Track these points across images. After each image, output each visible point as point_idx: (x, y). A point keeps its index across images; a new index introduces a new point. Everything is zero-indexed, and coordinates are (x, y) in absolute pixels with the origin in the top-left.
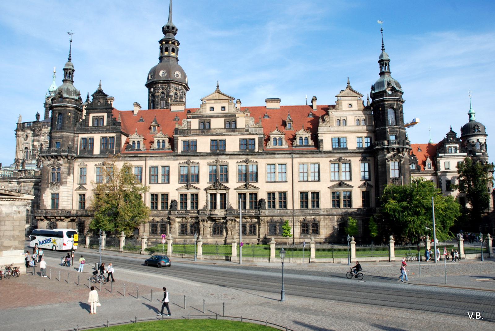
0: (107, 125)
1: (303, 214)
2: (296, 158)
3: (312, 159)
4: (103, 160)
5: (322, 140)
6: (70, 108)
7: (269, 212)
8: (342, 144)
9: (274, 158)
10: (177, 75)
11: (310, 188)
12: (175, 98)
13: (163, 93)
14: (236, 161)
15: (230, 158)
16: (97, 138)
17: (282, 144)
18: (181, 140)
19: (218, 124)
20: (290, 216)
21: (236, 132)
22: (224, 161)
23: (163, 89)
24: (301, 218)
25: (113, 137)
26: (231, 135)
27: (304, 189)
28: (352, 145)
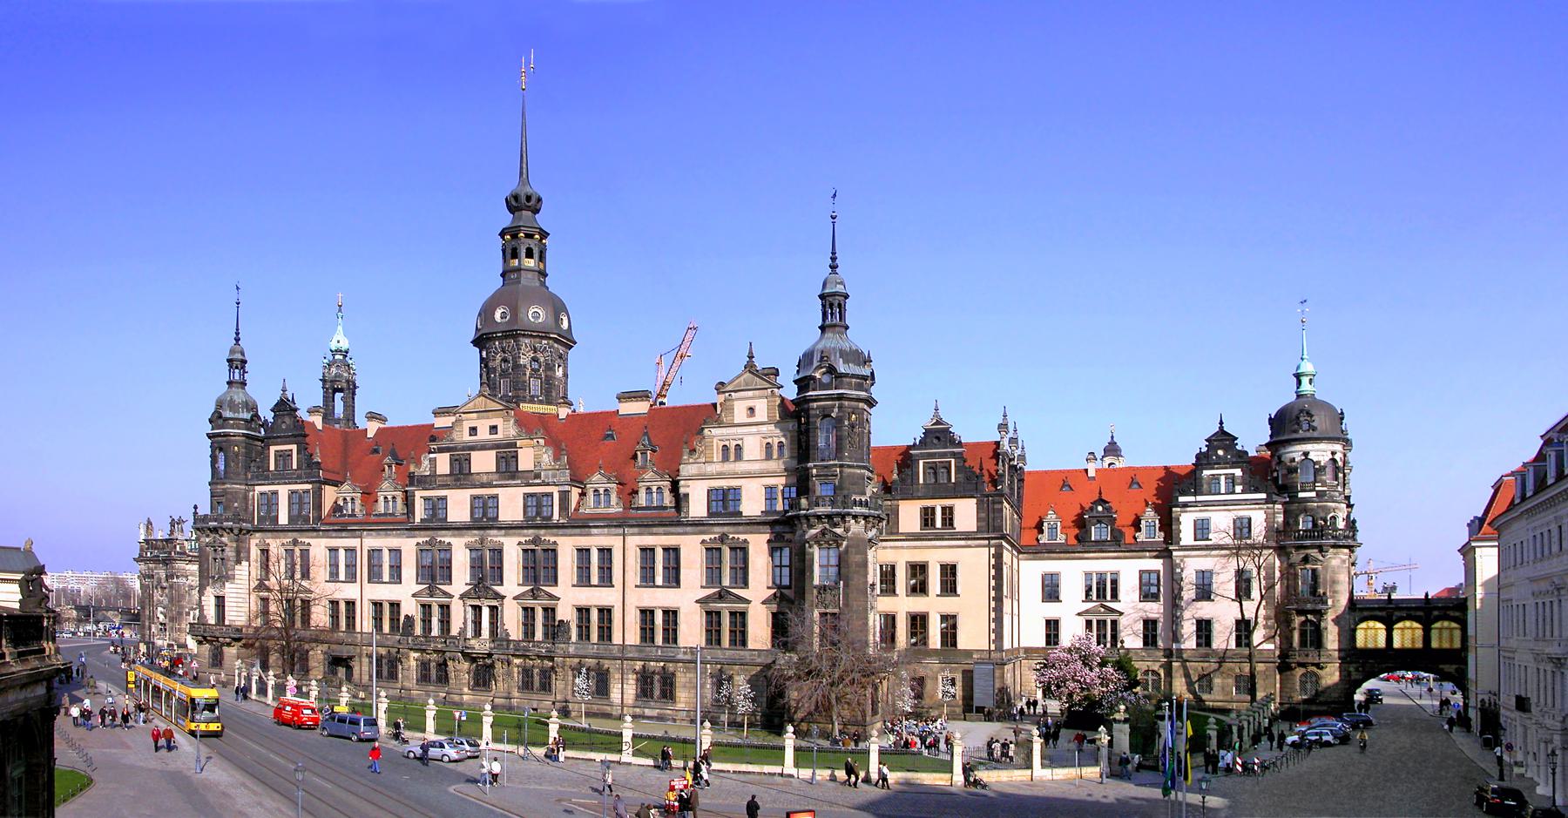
4: (295, 534)
5: (687, 495)
9: (589, 535)
11: (660, 598)
14: (516, 540)
16: (283, 491)
17: (608, 505)
19: (483, 462)
24: (638, 665)
25: (307, 491)
27: (647, 604)
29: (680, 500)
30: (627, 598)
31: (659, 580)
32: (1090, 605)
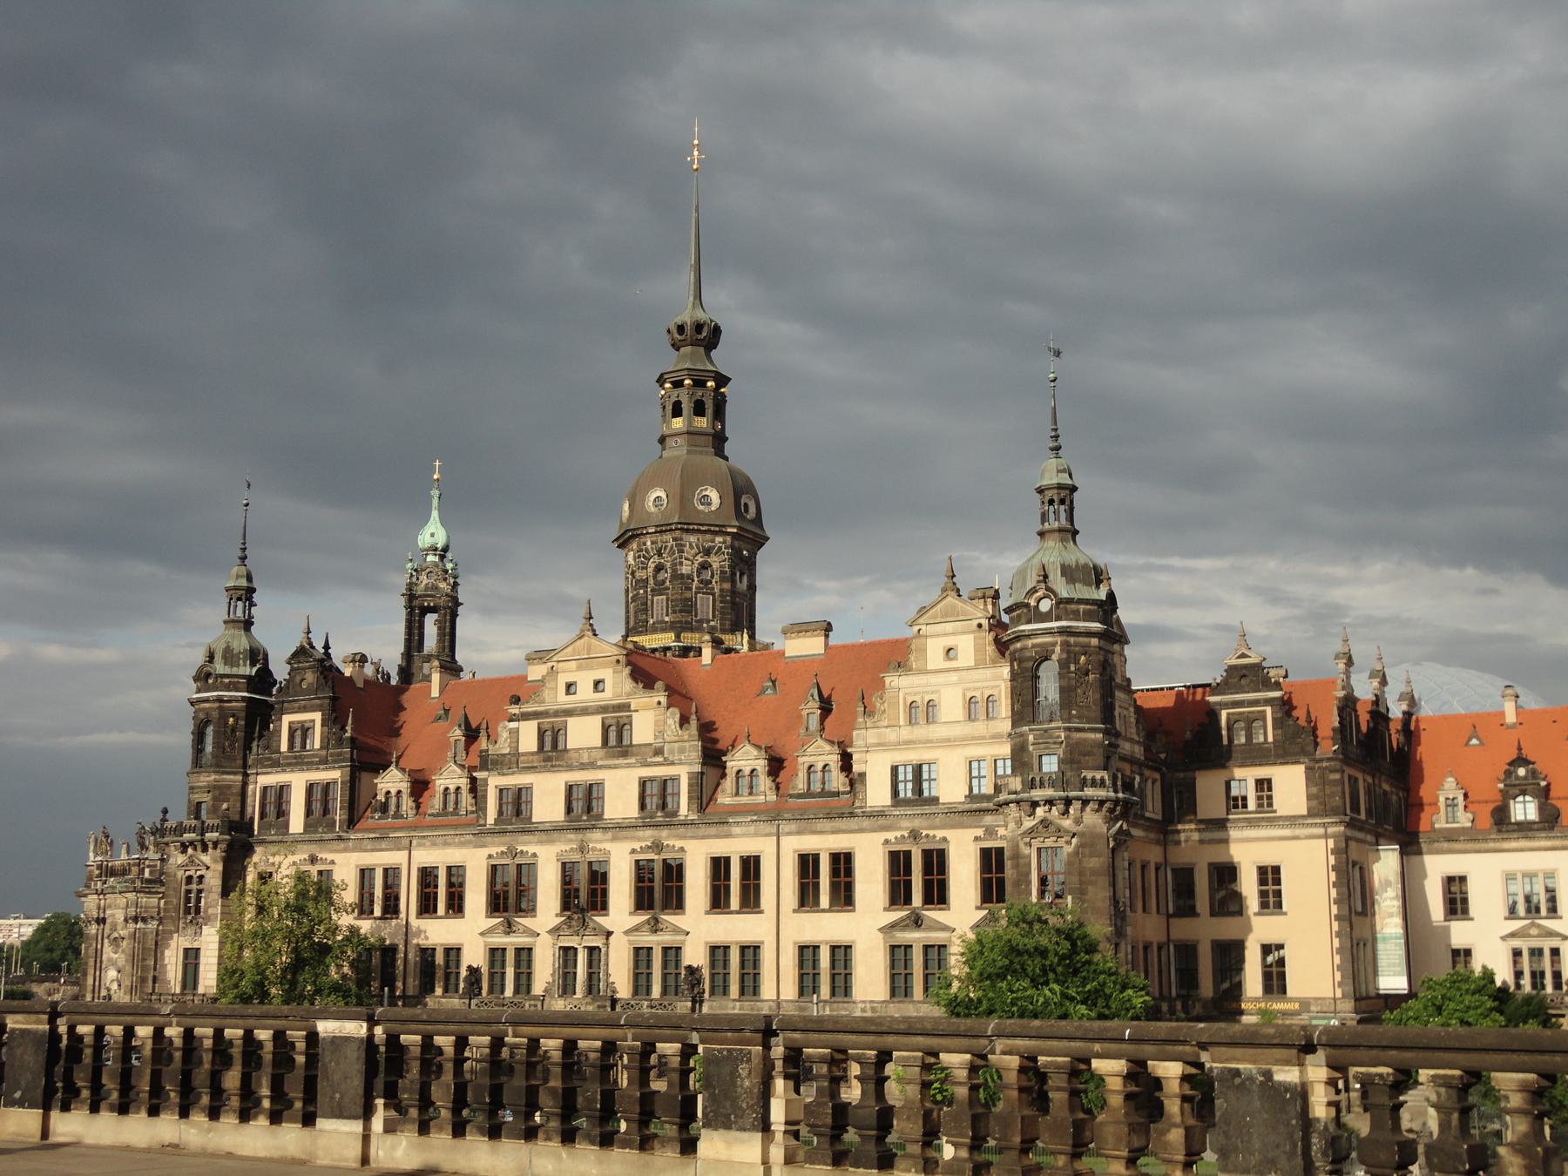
0: (322, 748)
2: (789, 834)
3: (831, 838)
4: (313, 848)
5: (862, 775)
8: (925, 785)
10: (705, 500)
11: (825, 927)
12: (701, 582)
13: (659, 568)
14: (627, 846)
15: (614, 839)
16: (298, 782)
18: (494, 782)
19: (583, 734)
22: (598, 846)
23: (660, 554)
26: (616, 767)
27: (808, 937)
29: (856, 782)
30: (779, 928)
31: (825, 900)
32: (1516, 925)
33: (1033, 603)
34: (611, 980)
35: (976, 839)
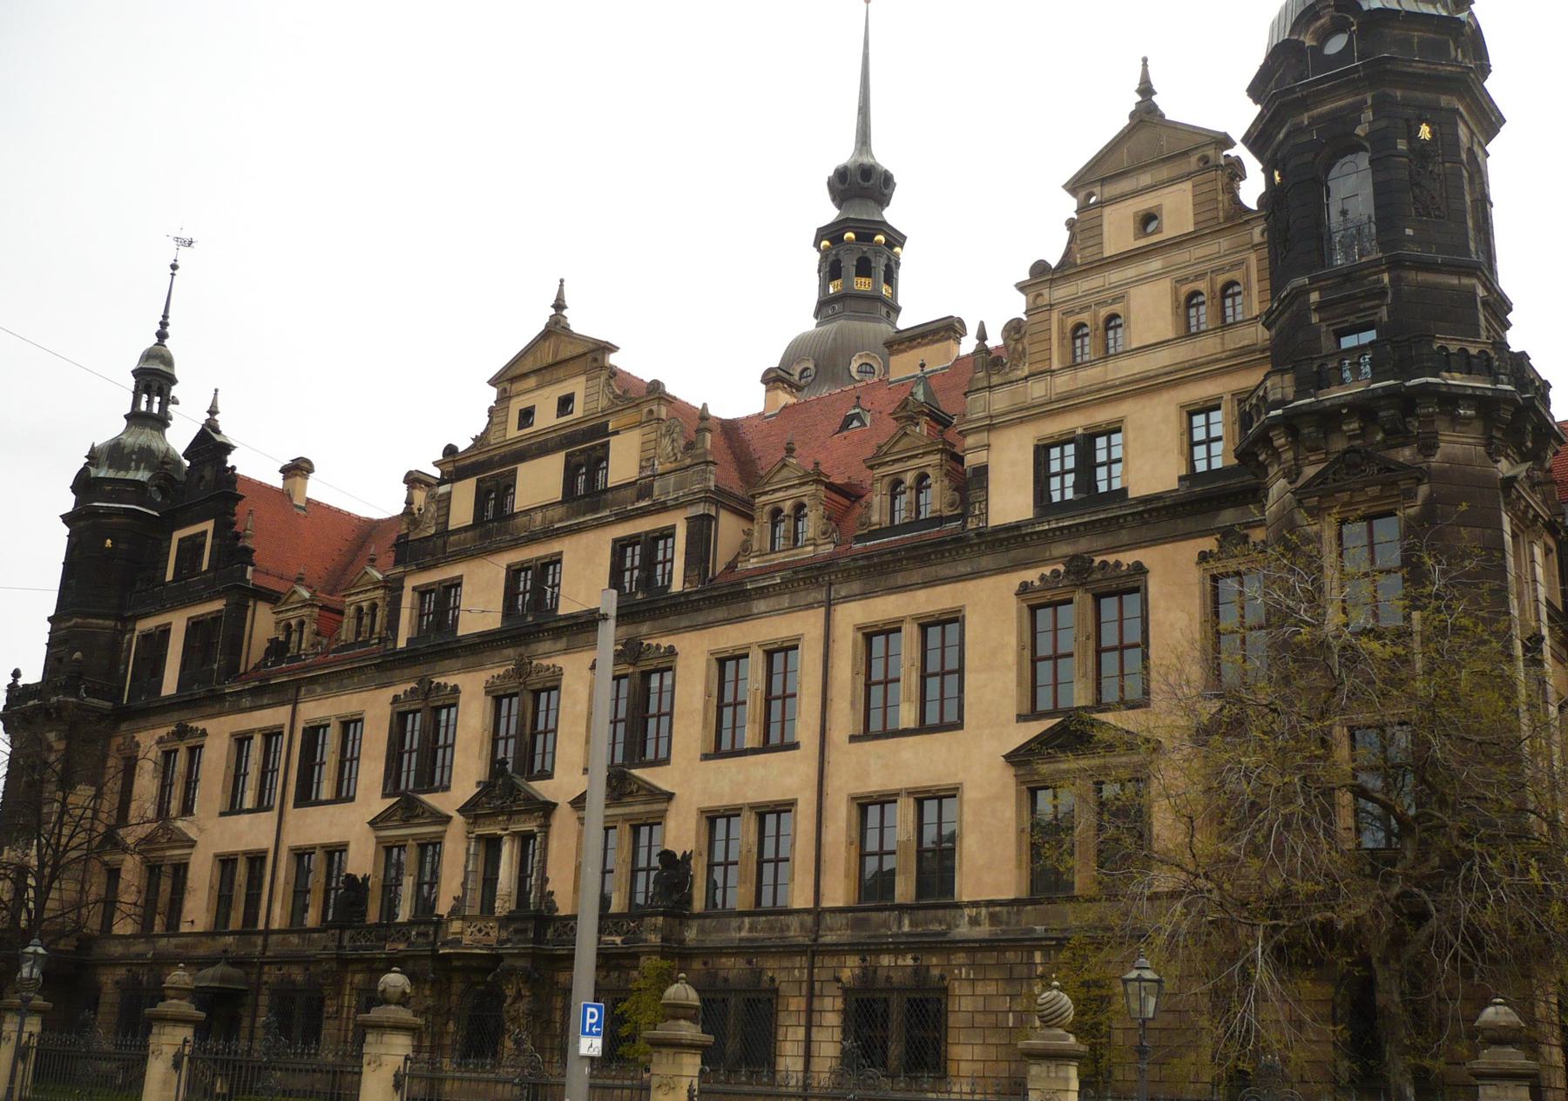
1: (862, 936)
3: (922, 595)
6: (115, 520)
7: (702, 930)
8: (1101, 473)
15: (566, 651)
16: (178, 622)
20: (791, 950)
21: (604, 508)
22: (545, 662)
24: (850, 968)
27: (875, 784)
28: (1147, 461)
29: (971, 485)
33: (1308, 41)
34: (549, 888)
35: (1204, 557)
